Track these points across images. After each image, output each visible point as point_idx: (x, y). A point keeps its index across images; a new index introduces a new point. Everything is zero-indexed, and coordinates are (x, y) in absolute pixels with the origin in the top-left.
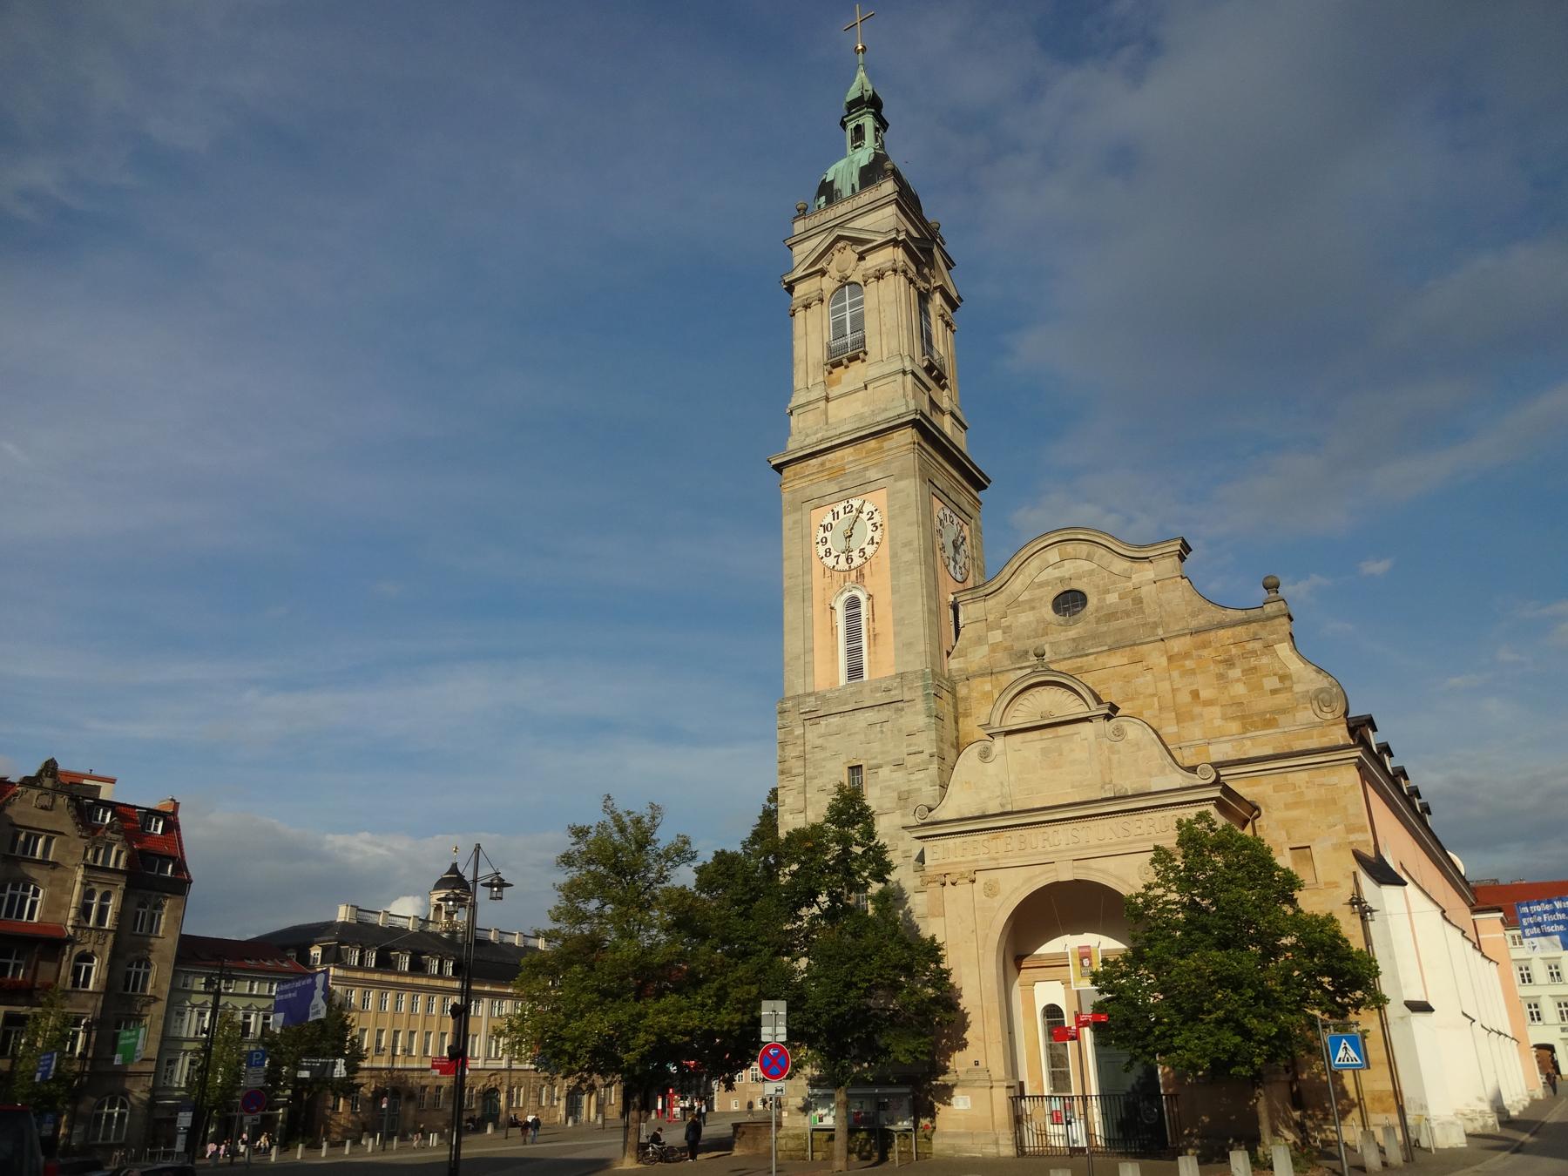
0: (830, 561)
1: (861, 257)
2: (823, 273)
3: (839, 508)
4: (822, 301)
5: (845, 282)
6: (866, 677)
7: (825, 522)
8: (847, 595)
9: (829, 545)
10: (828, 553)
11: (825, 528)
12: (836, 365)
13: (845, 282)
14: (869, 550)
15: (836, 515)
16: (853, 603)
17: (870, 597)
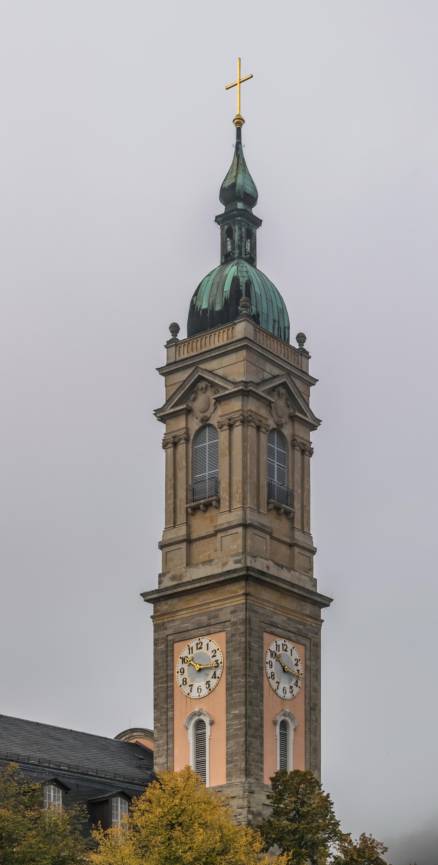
0: (186, 689)
1: (218, 400)
2: (189, 411)
3: (193, 643)
4: (187, 440)
5: (206, 424)
6: (207, 786)
7: (183, 656)
8: (196, 718)
9: (186, 675)
10: (185, 681)
11: (183, 660)
12: (195, 509)
13: (206, 424)
14: (213, 682)
15: (191, 650)
16: (200, 725)
17: (212, 723)
